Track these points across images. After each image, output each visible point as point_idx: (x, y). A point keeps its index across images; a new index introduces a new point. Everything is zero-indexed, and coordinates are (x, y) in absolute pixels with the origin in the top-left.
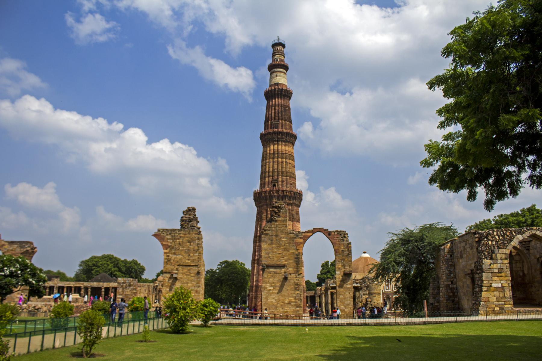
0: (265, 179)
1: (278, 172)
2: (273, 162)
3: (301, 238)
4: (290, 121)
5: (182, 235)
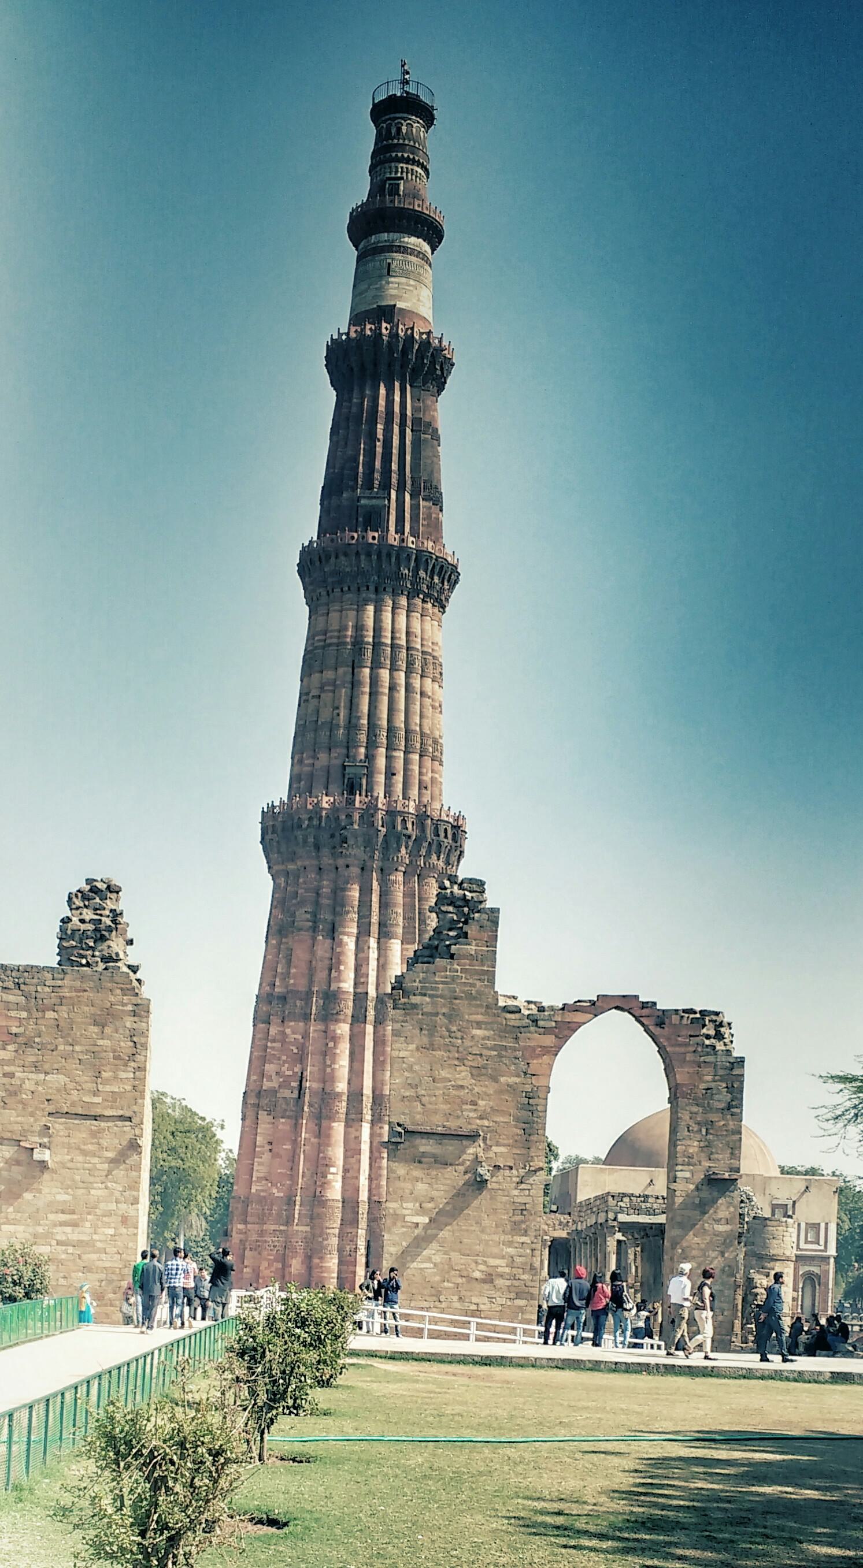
3: (547, 1031)
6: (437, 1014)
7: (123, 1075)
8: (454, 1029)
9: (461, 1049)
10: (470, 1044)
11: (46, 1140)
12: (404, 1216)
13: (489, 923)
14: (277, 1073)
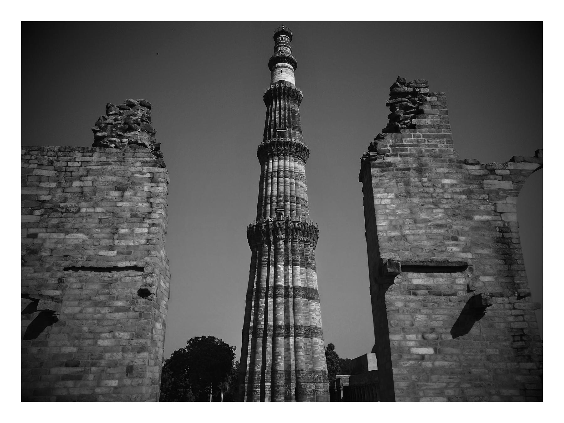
2: (278, 183)
6: (408, 169)
7: (138, 230)
8: (425, 180)
9: (434, 195)
10: (442, 191)
11: (58, 293)
12: (410, 347)
13: (438, 103)
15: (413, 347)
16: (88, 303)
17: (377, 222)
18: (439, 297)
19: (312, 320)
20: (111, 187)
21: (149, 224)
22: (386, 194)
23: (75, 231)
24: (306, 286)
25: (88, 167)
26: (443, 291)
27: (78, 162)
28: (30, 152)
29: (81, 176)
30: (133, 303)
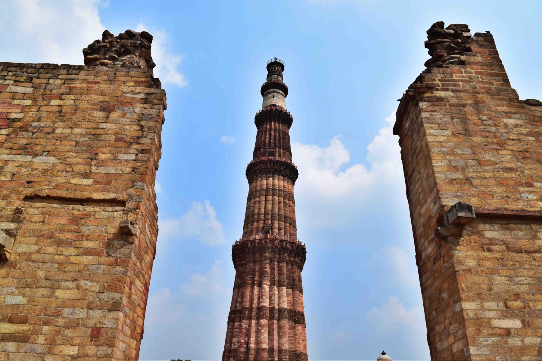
0: (253, 225)
1: (273, 214)
4: (291, 154)
5: (77, 85)
6: (464, 105)
7: (122, 156)
8: (485, 118)
10: (506, 131)
11: (13, 226)
12: (490, 319)
14: (238, 342)
15: (495, 319)
16: (49, 241)
17: (433, 161)
18: (520, 254)
19: (298, 345)
20: (95, 107)
21: (137, 150)
22: (440, 131)
23: (45, 154)
24: (292, 308)
25: (72, 85)
26: (523, 247)
27: (61, 79)
28: (9, 69)
29: (63, 94)
30: (109, 245)
